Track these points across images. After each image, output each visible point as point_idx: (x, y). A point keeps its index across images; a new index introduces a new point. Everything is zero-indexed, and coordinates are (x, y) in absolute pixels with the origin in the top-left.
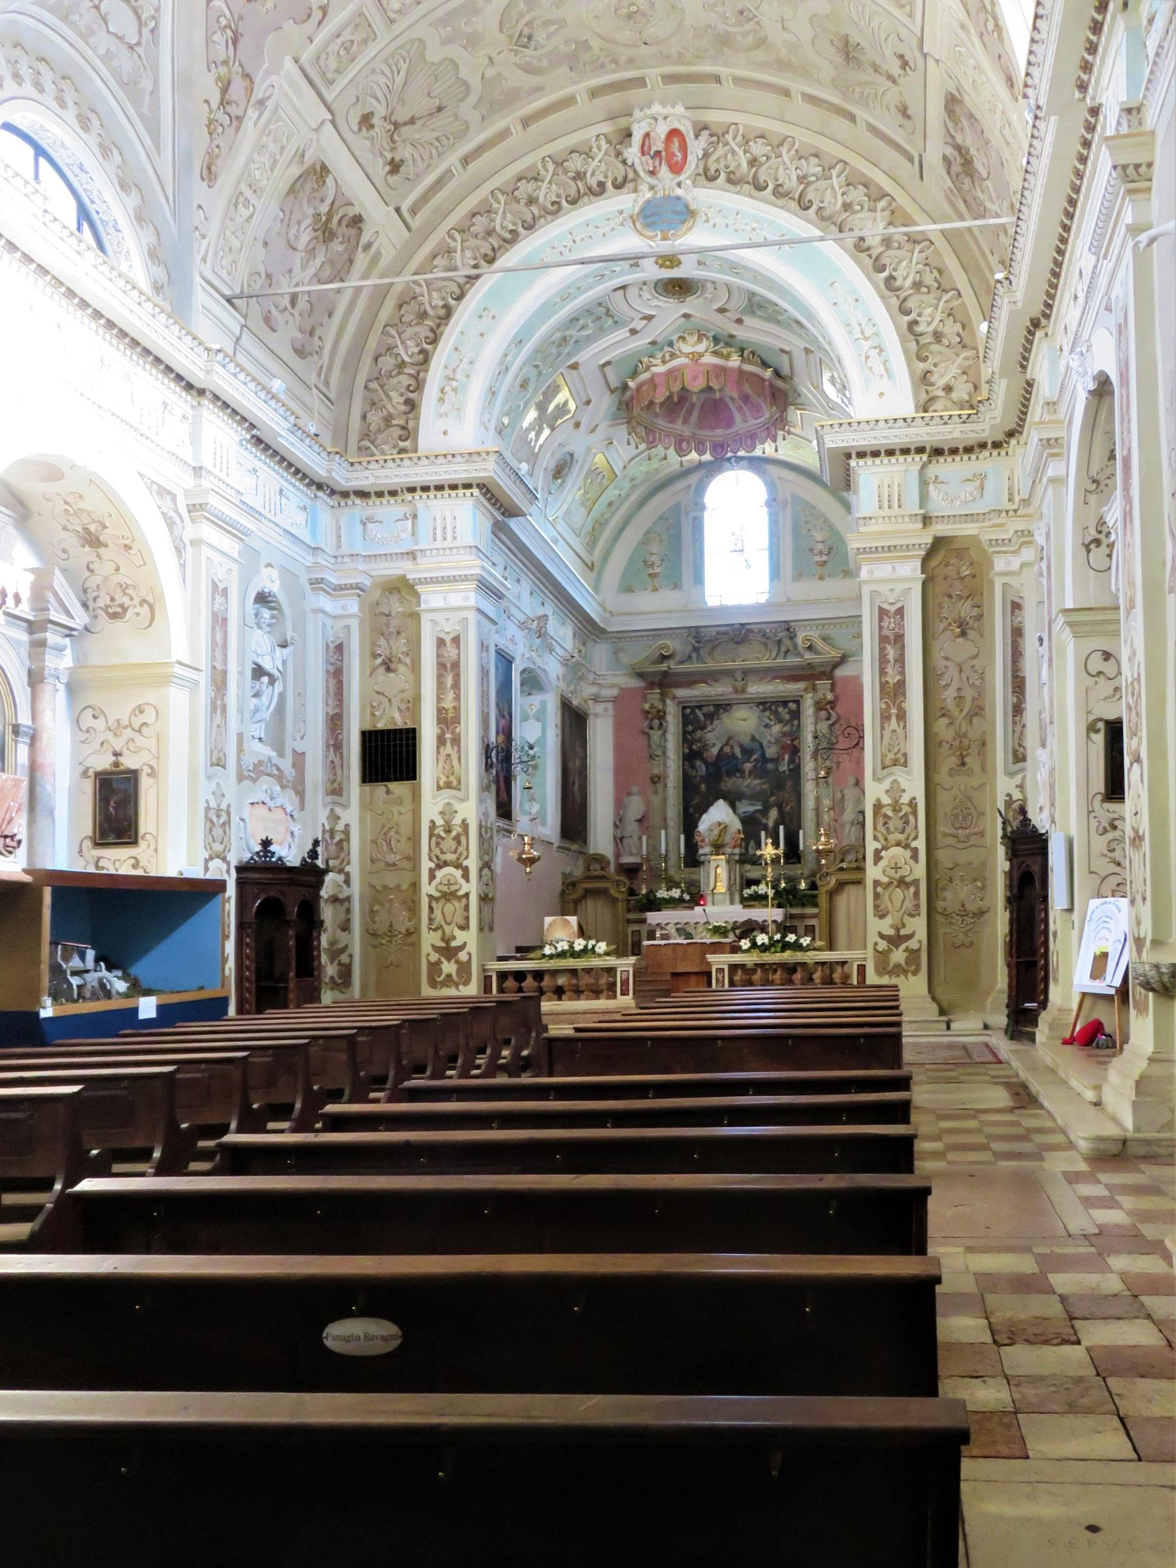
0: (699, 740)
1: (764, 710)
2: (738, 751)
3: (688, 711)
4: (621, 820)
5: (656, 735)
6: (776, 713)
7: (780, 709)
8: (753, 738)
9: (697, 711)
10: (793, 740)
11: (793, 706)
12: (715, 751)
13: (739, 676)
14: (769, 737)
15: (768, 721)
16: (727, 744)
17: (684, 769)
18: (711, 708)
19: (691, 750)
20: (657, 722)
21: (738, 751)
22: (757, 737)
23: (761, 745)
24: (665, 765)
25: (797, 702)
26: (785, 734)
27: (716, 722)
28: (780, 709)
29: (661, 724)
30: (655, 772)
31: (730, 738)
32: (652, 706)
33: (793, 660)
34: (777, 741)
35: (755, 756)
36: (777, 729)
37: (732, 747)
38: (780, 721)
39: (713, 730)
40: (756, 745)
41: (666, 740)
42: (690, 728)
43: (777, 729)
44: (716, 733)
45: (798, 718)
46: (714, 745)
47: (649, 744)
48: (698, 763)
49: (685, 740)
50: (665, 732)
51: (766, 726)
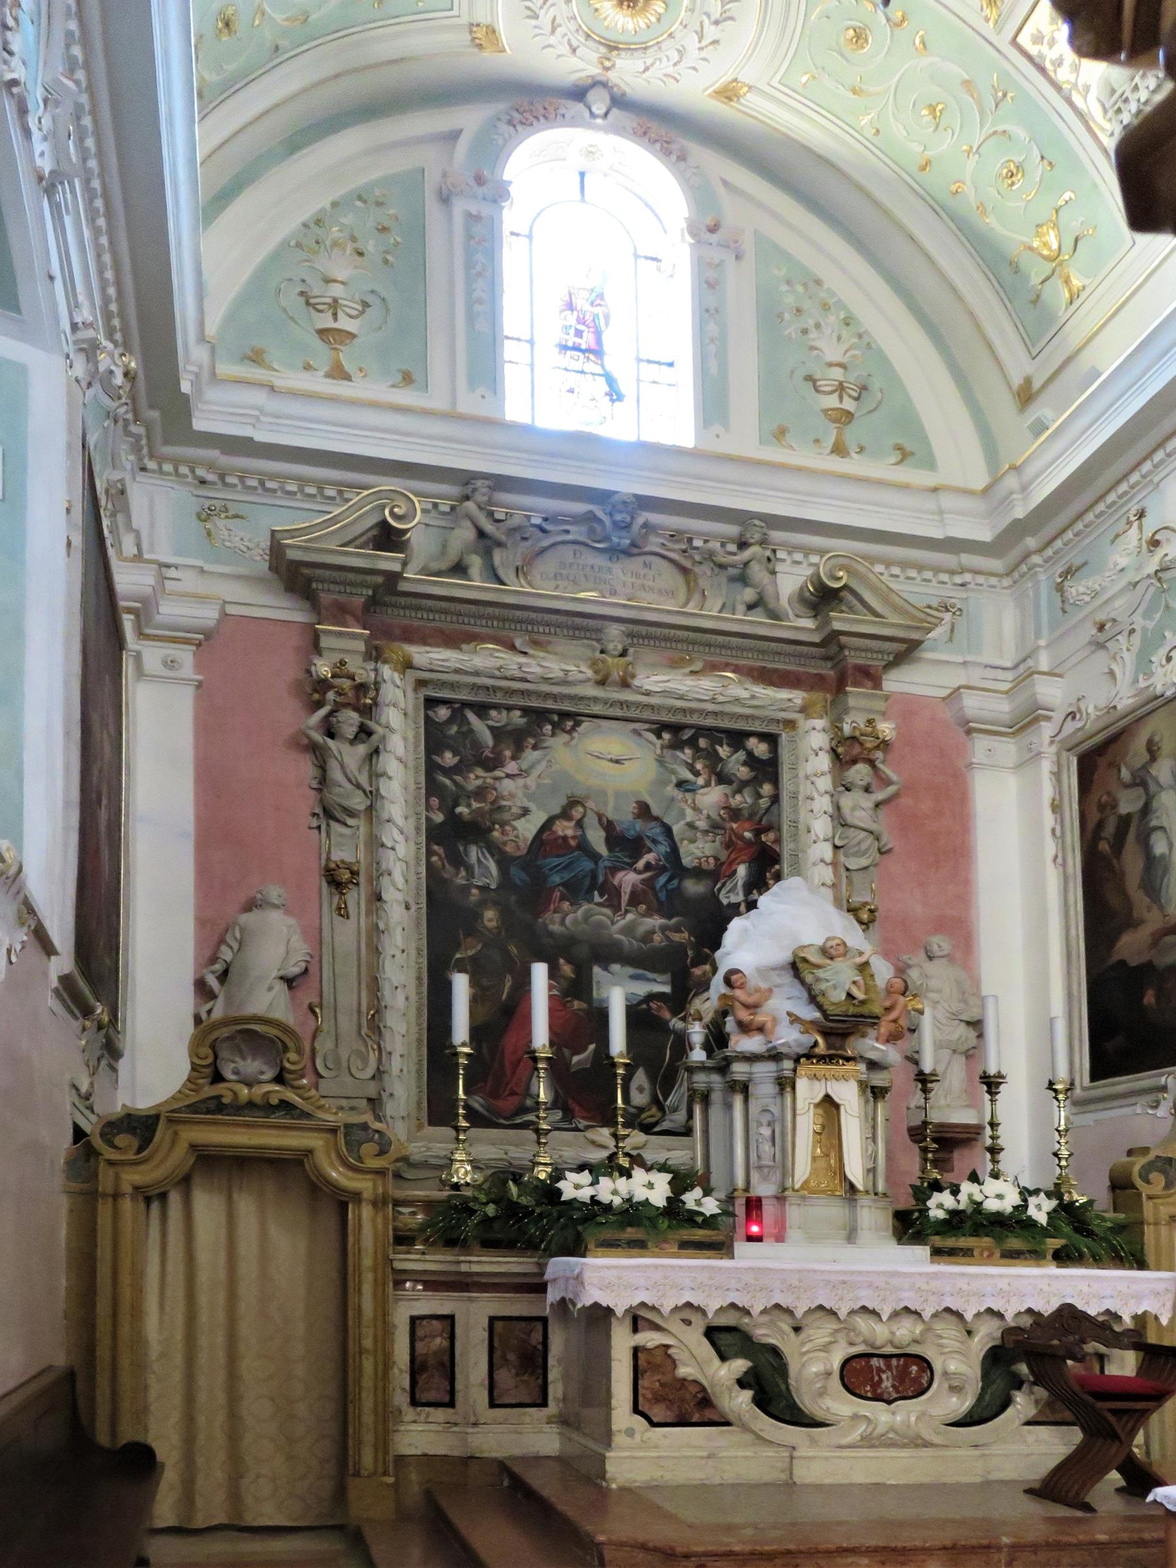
0: (480, 793)
1: (677, 745)
2: (596, 838)
3: (443, 713)
4: (224, 976)
5: (350, 756)
6: (713, 758)
7: (723, 751)
8: (644, 811)
9: (471, 716)
10: (758, 832)
11: (760, 749)
12: (527, 829)
13: (614, 634)
14: (690, 815)
15: (690, 776)
16: (565, 814)
18: (517, 718)
19: (452, 817)
20: (350, 720)
21: (596, 838)
22: (655, 810)
23: (668, 831)
24: (375, 844)
25: (771, 739)
26: (735, 814)
27: (530, 756)
28: (723, 751)
29: (364, 733)
30: (338, 855)
31: (573, 802)
32: (340, 670)
33: (758, 623)
34: (715, 827)
35: (650, 857)
36: (712, 797)
37: (580, 824)
39: (522, 773)
40: (655, 831)
41: (376, 775)
42: (449, 759)
43: (712, 797)
44: (531, 781)
45: (775, 780)
46: (525, 812)
47: (323, 780)
49: (432, 788)
50: (377, 751)
51: (680, 784)
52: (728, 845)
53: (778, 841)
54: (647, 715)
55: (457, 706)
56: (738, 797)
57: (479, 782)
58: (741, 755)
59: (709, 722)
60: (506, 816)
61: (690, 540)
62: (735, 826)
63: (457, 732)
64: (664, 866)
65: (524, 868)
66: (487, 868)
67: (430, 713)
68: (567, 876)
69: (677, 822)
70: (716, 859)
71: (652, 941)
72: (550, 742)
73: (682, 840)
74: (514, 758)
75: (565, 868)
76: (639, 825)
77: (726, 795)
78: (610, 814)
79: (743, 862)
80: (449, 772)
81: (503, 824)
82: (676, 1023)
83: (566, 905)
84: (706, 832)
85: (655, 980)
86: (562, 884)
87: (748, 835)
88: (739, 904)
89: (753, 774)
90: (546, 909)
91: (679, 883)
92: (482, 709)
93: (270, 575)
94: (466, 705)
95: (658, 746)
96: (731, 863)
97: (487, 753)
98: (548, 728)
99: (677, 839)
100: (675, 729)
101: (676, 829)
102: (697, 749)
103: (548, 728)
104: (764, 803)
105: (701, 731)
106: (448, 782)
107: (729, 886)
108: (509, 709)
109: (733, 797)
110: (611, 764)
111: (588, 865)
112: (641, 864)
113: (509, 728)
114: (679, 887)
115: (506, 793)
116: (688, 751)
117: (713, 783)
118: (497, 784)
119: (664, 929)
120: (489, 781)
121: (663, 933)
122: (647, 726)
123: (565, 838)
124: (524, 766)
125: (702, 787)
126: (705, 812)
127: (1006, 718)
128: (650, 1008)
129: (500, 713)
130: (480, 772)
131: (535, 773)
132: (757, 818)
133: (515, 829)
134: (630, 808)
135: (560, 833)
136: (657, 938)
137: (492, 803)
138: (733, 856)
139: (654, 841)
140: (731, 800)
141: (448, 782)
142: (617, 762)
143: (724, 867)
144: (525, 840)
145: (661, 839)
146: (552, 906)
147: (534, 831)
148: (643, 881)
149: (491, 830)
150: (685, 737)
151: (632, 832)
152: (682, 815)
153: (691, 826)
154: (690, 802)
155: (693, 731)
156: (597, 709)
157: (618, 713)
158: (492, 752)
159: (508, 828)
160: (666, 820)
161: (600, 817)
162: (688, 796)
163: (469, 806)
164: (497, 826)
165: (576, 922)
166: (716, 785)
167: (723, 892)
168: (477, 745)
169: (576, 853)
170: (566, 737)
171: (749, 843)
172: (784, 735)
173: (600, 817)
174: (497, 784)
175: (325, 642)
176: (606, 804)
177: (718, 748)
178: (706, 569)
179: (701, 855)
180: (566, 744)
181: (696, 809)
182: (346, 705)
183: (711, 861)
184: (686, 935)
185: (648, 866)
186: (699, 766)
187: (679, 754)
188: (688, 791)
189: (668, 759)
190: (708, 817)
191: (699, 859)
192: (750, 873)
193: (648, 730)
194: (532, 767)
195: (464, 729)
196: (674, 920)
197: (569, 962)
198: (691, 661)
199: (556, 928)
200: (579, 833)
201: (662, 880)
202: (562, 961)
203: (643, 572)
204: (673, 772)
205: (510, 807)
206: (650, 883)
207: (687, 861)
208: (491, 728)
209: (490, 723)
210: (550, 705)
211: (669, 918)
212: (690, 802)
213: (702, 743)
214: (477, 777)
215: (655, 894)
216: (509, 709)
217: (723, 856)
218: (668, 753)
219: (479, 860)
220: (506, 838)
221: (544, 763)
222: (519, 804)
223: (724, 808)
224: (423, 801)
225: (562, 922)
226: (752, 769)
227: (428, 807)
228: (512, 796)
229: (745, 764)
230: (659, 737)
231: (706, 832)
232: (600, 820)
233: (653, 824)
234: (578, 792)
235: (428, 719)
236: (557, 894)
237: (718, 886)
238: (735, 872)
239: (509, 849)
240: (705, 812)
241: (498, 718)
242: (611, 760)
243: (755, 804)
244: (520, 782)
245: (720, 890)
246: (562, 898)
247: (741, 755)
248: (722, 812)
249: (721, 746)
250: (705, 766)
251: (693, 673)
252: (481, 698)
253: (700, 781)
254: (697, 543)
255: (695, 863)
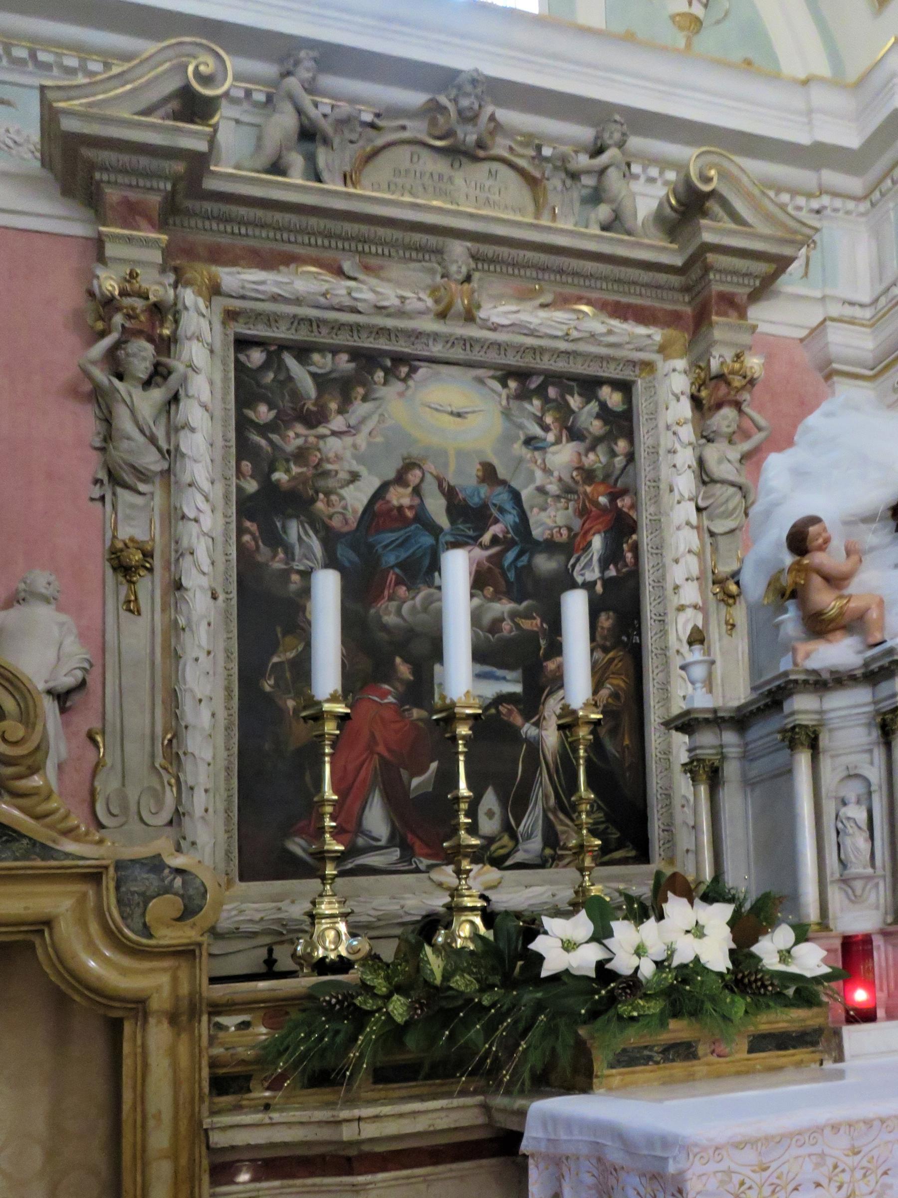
0: (301, 455)
1: (523, 395)
3: (257, 357)
7: (574, 402)
8: (489, 474)
9: (290, 361)
10: (614, 496)
11: (613, 399)
15: (537, 431)
16: (400, 479)
17: (241, 548)
19: (269, 488)
23: (516, 496)
25: (625, 387)
26: (588, 475)
28: (574, 402)
31: (409, 465)
34: (568, 491)
35: (496, 529)
37: (417, 491)
38: (575, 435)
39: (351, 430)
40: (502, 497)
42: (263, 413)
44: (361, 439)
45: (630, 435)
46: (355, 477)
48: (294, 530)
51: (529, 441)
52: (583, 512)
53: (634, 506)
54: (493, 357)
55: (273, 348)
56: (592, 456)
57: (300, 442)
58: (593, 406)
59: (560, 366)
60: (331, 483)
61: (539, 148)
62: (589, 489)
63: (273, 380)
64: (512, 538)
65: (354, 547)
66: (310, 548)
67: (242, 357)
68: (403, 555)
69: (526, 487)
70: (570, 529)
71: (500, 630)
72: (382, 391)
73: (532, 508)
74: (341, 411)
75: (401, 545)
76: (484, 490)
77: (579, 454)
78: (452, 479)
79: (598, 532)
80: (264, 429)
81: (327, 494)
82: (528, 730)
83: (402, 590)
84: (558, 497)
85: (504, 679)
86: (400, 565)
87: (603, 500)
88: (595, 583)
89: (608, 428)
90: (379, 596)
91: (530, 561)
92: (303, 352)
93: (45, 173)
94: (284, 346)
95: (504, 396)
96: (586, 533)
97: (310, 406)
98: (380, 375)
99: (526, 506)
100: (522, 375)
101: (525, 494)
102: (546, 400)
103: (380, 375)
104: (619, 461)
105: (552, 378)
106: (263, 442)
107: (583, 561)
108: (335, 351)
109: (586, 456)
110: (451, 418)
111: (427, 540)
112: (486, 538)
113: (334, 375)
114: (529, 567)
115: (331, 455)
116: (537, 402)
117: (564, 439)
118: (321, 443)
119: (513, 615)
120: (312, 439)
121: (513, 620)
122: (491, 373)
123: (400, 508)
124: (353, 422)
125: (553, 444)
126: (556, 474)
127: (869, 357)
128: (498, 711)
129: (324, 357)
130: (300, 428)
131: (366, 429)
132: (612, 480)
133: (342, 498)
134: (475, 470)
135: (395, 502)
136: (507, 626)
137: (316, 467)
138: (587, 526)
139: (501, 510)
140: (584, 458)
141: (263, 442)
142: (459, 415)
143: (578, 539)
144: (355, 511)
145: (508, 506)
146: (386, 593)
147: (365, 501)
148: (490, 558)
149: (313, 500)
150: (533, 386)
151: (476, 500)
152: (531, 478)
153: (541, 490)
154: (539, 462)
155: (541, 378)
156: (436, 349)
157: (457, 353)
158: (315, 404)
159: (334, 498)
160: (515, 484)
161: (440, 481)
162: (537, 454)
163: (288, 471)
164: (321, 496)
165: (413, 608)
166: (568, 441)
167: (578, 568)
168: (296, 395)
169: (413, 527)
170: (399, 386)
171: (604, 510)
172: (639, 382)
173: (440, 481)
174: (321, 443)
175: (111, 250)
176: (446, 465)
177: (569, 398)
178: (556, 182)
179: (552, 524)
180: (401, 395)
181: (547, 471)
182: (138, 333)
183: (564, 532)
184: (538, 621)
185: (495, 540)
186: (549, 420)
187: (527, 406)
188: (536, 449)
189: (515, 412)
190: (560, 479)
191: (551, 529)
192: (606, 545)
193: (493, 377)
194: (363, 420)
195: (282, 377)
196: (525, 604)
197: (406, 660)
198: (541, 291)
199: (390, 619)
200: (417, 501)
201: (511, 556)
202: (398, 660)
203: (488, 183)
204: (521, 427)
205: (337, 472)
206: (498, 560)
207: (538, 533)
208: (314, 376)
209: (313, 369)
210: (382, 344)
211: (519, 601)
212: (539, 462)
213: (552, 392)
214: (297, 435)
215: (504, 574)
216: (335, 351)
217: (577, 524)
218: (514, 404)
219: (300, 539)
220: (332, 510)
221: (375, 418)
222: (347, 467)
223: (577, 469)
224: (233, 463)
225: (399, 612)
226: (606, 422)
227: (239, 472)
228: (338, 458)
229: (598, 416)
230: (505, 385)
231: (558, 497)
232: (440, 486)
233: (499, 489)
234: (415, 452)
235: (238, 364)
236: (392, 577)
237: (572, 561)
238: (590, 544)
239: (336, 523)
240: (556, 474)
241: (321, 362)
242: (451, 413)
243: (610, 465)
244: (348, 440)
245: (574, 566)
246: (399, 582)
247: (593, 406)
248: (575, 474)
249: (573, 396)
250: (556, 420)
251: (543, 306)
252: (302, 335)
253: (551, 437)
254: (547, 152)
255: (547, 535)
